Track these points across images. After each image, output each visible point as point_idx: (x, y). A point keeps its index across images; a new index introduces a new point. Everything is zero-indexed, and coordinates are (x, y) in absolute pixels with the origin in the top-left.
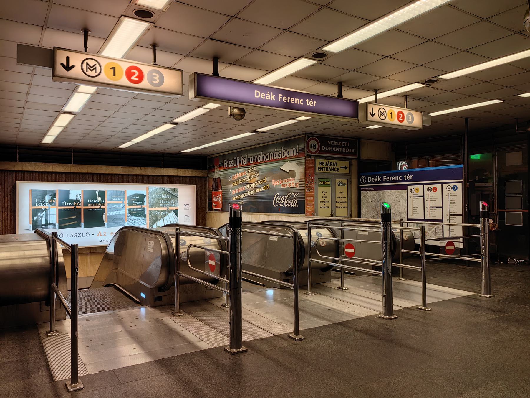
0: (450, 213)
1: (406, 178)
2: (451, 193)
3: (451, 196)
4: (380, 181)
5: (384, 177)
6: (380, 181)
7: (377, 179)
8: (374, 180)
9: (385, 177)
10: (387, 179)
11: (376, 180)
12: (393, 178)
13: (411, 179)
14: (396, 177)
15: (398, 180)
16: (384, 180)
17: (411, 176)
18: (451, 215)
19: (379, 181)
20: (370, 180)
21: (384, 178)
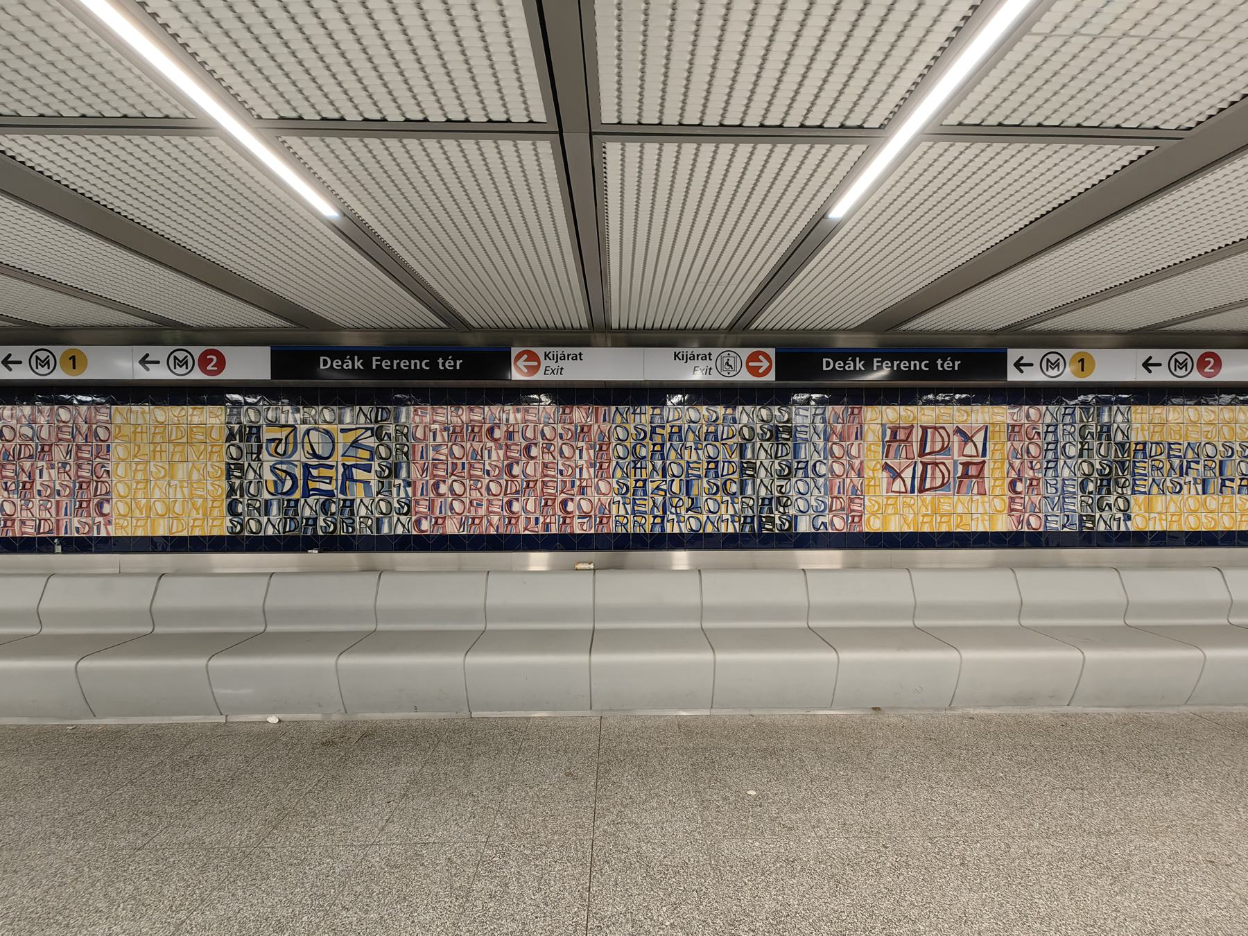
1: (443, 364)
4: (362, 368)
5: (374, 358)
6: (362, 368)
9: (377, 360)
10: (383, 364)
11: (347, 366)
12: (402, 365)
13: (458, 368)
14: (413, 362)
16: (374, 367)
17: (458, 362)
19: (356, 368)
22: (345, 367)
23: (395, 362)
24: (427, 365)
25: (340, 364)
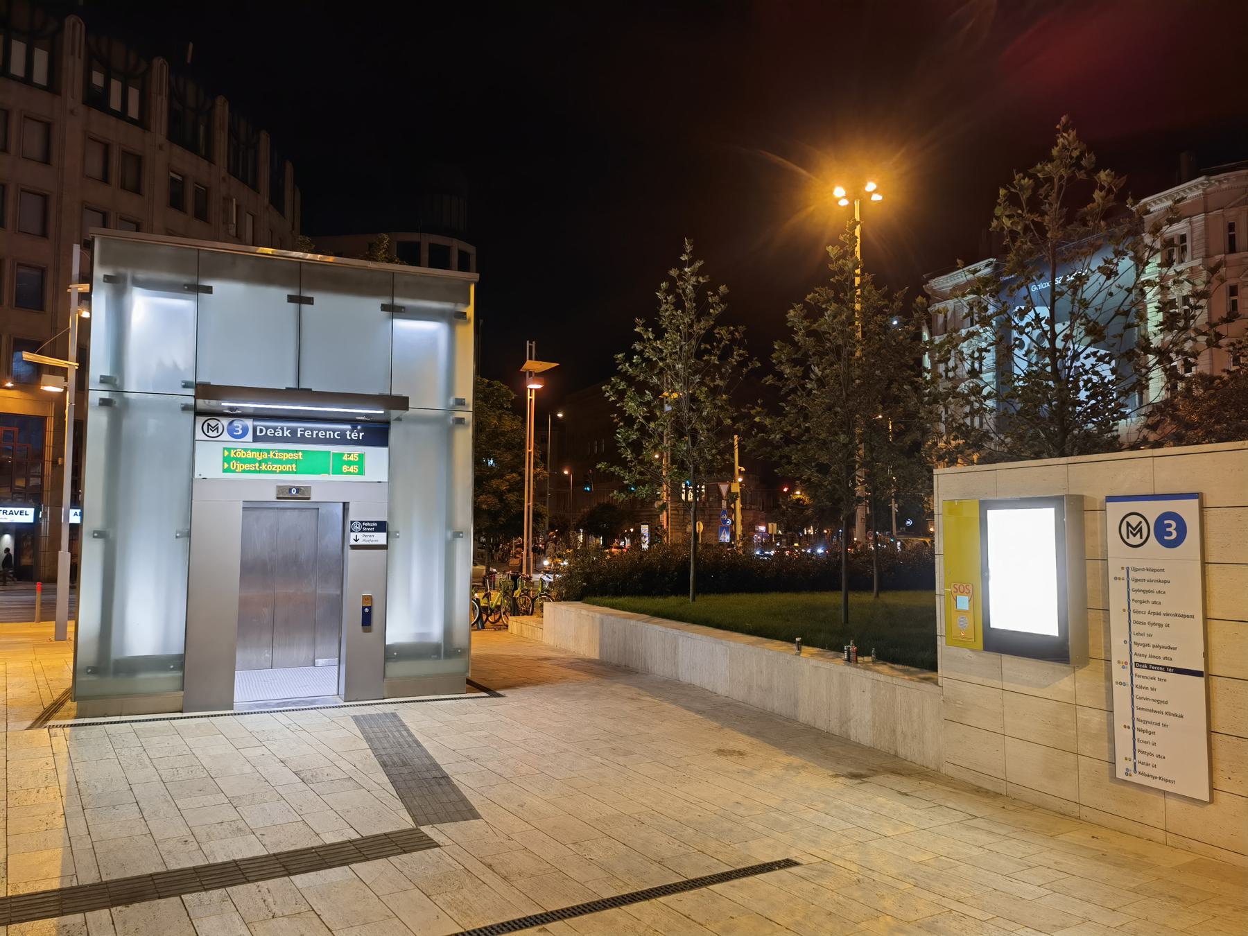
0: (1135, 659)
1: (350, 436)
2: (1136, 570)
3: (1137, 581)
4: (289, 435)
6: (289, 435)
8: (274, 434)
9: (301, 431)
10: (306, 434)
13: (361, 438)
15: (332, 437)
16: (299, 435)
17: (361, 434)
18: (1140, 665)
22: (276, 434)
24: (338, 435)
25: (273, 432)
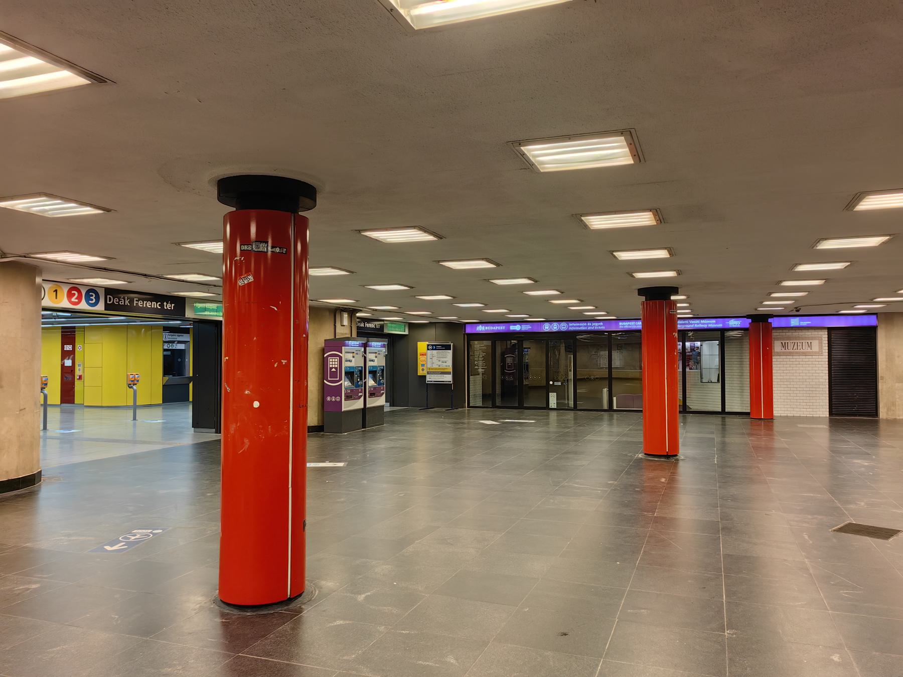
1: (166, 307)
4: (129, 304)
6: (129, 304)
7: (123, 301)
8: (119, 302)
10: (139, 303)
11: (122, 303)
14: (153, 303)
16: (135, 305)
17: (173, 305)
20: (110, 301)
21: (135, 302)
23: (145, 302)
